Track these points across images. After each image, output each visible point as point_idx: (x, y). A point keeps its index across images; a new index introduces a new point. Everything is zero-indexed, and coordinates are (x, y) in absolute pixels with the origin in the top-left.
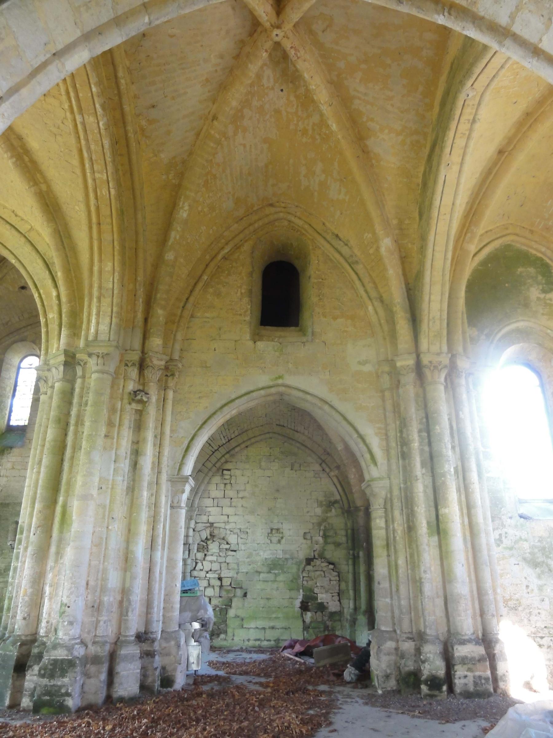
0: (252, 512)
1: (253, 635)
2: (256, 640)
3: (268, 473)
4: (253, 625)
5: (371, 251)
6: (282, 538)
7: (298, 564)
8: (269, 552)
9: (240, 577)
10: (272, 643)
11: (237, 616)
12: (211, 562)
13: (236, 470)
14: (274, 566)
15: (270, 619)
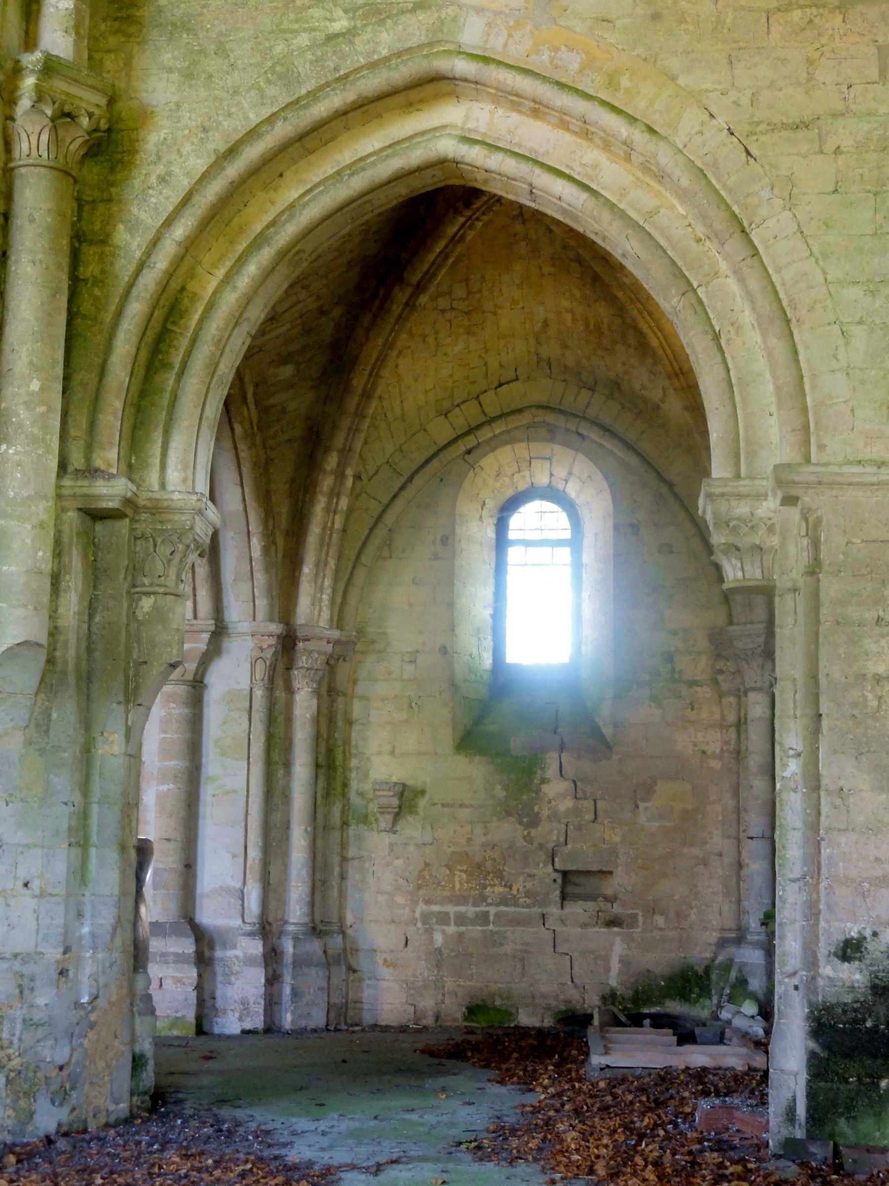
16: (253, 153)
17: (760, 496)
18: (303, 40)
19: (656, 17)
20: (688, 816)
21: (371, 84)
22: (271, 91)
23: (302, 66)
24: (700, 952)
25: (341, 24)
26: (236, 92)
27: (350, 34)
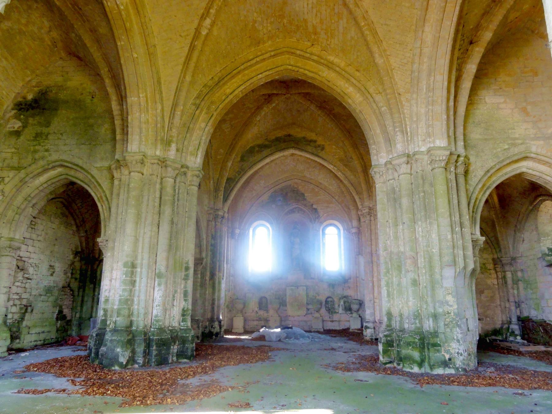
0: (43, 253)
1: (33, 338)
2: (35, 341)
3: (54, 226)
4: (34, 332)
5: (218, 157)
6: (54, 272)
7: (59, 290)
8: (47, 281)
9: (31, 298)
10: (42, 342)
11: (27, 326)
12: (18, 286)
13: (38, 220)
14: (49, 290)
15: (43, 326)
16: (492, 171)
18: (499, 150)
20: (492, 297)
21: (515, 158)
22: (495, 159)
24: (498, 326)
25: (507, 147)
26: (487, 159)
27: (509, 149)
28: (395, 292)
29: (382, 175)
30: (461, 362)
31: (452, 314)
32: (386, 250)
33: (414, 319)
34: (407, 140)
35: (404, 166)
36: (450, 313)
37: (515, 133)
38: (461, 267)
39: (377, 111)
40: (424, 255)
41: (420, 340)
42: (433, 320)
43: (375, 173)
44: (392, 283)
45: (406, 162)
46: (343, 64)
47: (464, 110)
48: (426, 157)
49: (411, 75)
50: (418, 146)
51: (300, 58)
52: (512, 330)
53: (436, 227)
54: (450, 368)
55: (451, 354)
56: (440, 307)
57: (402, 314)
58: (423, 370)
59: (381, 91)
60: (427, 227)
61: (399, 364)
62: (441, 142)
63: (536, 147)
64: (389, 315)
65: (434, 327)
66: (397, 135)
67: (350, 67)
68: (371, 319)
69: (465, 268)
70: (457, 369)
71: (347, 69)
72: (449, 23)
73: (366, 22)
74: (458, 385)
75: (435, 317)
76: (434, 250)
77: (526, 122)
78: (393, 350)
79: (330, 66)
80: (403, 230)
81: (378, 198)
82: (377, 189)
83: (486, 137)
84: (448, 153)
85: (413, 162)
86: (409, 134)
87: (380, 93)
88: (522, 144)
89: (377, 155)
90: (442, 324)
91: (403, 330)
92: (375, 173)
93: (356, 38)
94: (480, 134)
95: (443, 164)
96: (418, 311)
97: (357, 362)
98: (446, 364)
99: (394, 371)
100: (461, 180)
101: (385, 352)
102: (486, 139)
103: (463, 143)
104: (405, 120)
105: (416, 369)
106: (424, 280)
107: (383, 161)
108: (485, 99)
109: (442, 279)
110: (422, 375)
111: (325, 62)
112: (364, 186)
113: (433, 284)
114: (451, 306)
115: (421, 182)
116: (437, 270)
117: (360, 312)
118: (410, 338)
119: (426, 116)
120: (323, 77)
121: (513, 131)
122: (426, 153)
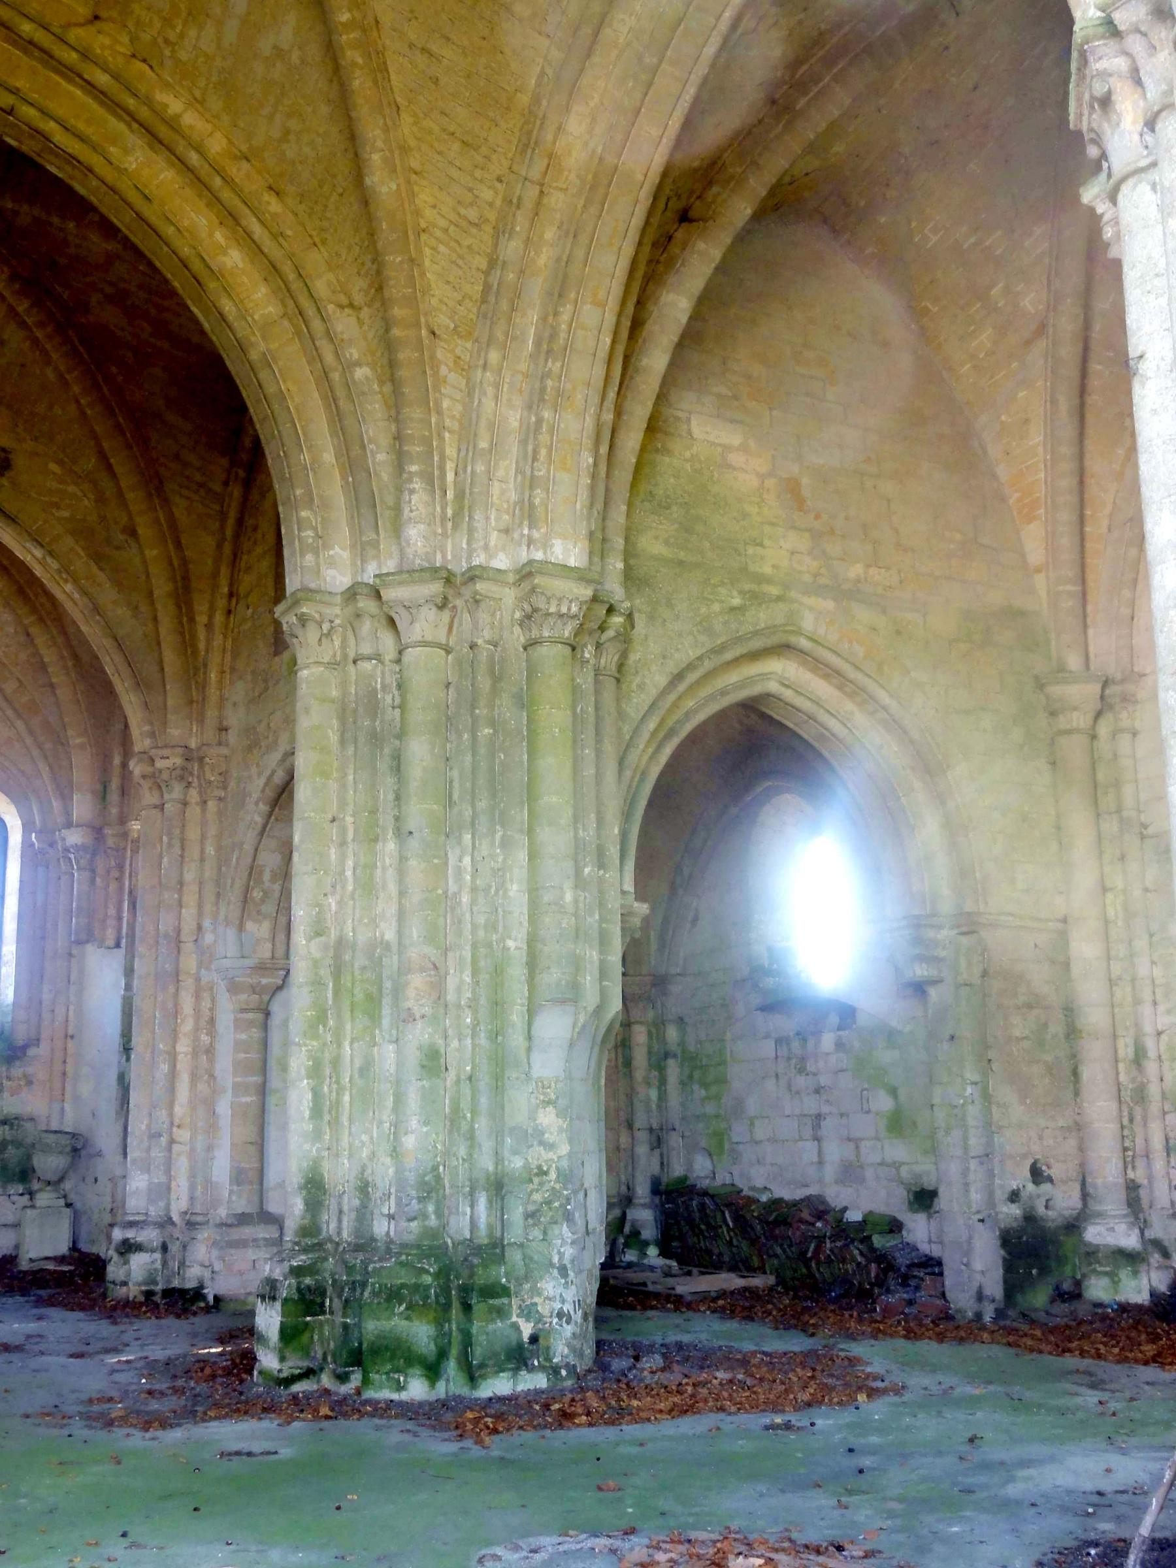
16: (692, 677)
17: (940, 927)
18: (716, 607)
19: (898, 632)
22: (702, 638)
23: (718, 626)
25: (737, 601)
26: (680, 635)
27: (741, 609)
28: (347, 1098)
29: (329, 634)
30: (568, 1345)
31: (553, 1175)
32: (319, 931)
33: (421, 1200)
34: (444, 518)
35: (429, 614)
36: (546, 1173)
37: (762, 558)
38: (591, 1009)
39: (336, 376)
40: (474, 962)
41: (436, 1276)
42: (490, 1202)
43: (303, 620)
44: (336, 1062)
45: (439, 601)
46: (216, 145)
47: (638, 447)
48: (509, 596)
49: (487, 273)
50: (486, 547)
51: (25, 51)
52: (633, 1226)
53: (522, 856)
54: (531, 1369)
55: (540, 1319)
56: (515, 1153)
57: (367, 1184)
58: (441, 1390)
59: (358, 299)
60: (492, 857)
61: (343, 1378)
62: (568, 551)
63: (814, 617)
64: (315, 1189)
65: (490, 1227)
66: (412, 492)
67: (245, 165)
68: (155, 1212)
69: (599, 1010)
70: (555, 1370)
71: (239, 171)
72: (655, 132)
73: (357, 15)
74: (590, 1425)
75: (498, 1187)
76: (511, 944)
77: (794, 528)
78: (321, 1324)
79: (159, 135)
80: (402, 859)
81: (304, 723)
82: (303, 689)
83: (682, 555)
84: (588, 592)
85: (459, 603)
86: (450, 494)
87: (351, 305)
88: (779, 599)
89: (317, 554)
90: (516, 1214)
91: (364, 1244)
92: (303, 620)
93: (295, 57)
94: (667, 543)
95: (567, 632)
96: (435, 1168)
97: (163, 1386)
98: (519, 1356)
99: (344, 1408)
100: (608, 696)
101: (289, 1335)
102: (681, 563)
103: (620, 565)
104: (441, 438)
105: (417, 1389)
106: (461, 1053)
107: (338, 579)
108: (689, 421)
109: (529, 1050)
110: (444, 1404)
111: (144, 113)
112: (170, 657)
113: (500, 1067)
114: (551, 1147)
115: (484, 683)
116: (517, 1016)
117: (68, 1185)
118: (403, 1272)
119: (524, 442)
120: (123, 171)
121: (759, 550)
122: (511, 578)
